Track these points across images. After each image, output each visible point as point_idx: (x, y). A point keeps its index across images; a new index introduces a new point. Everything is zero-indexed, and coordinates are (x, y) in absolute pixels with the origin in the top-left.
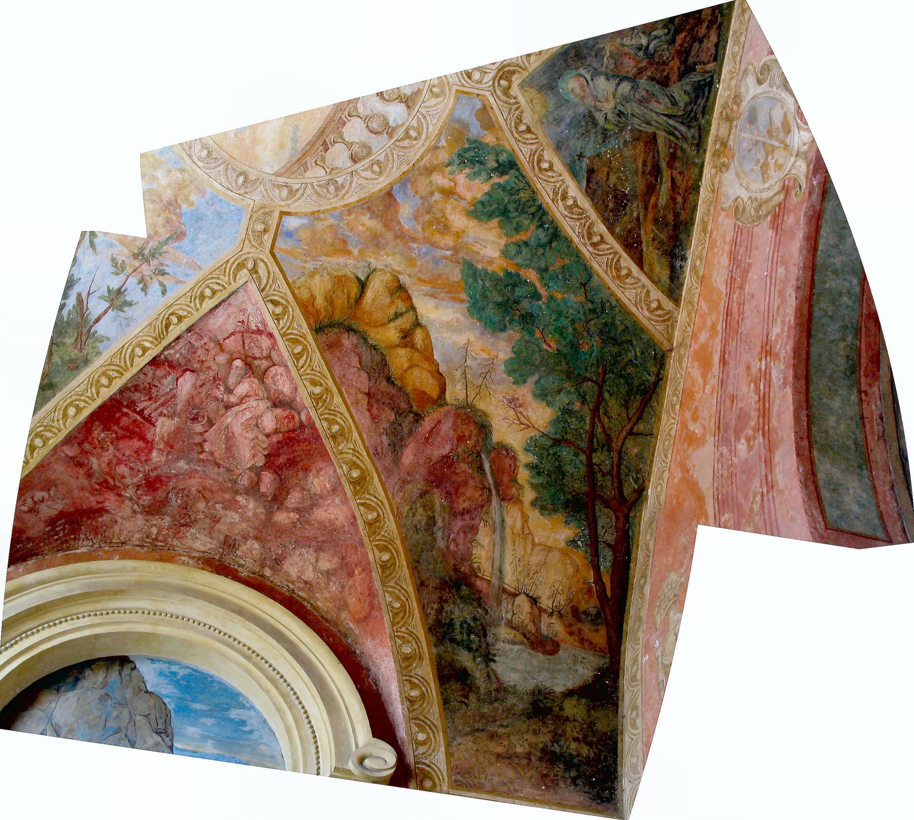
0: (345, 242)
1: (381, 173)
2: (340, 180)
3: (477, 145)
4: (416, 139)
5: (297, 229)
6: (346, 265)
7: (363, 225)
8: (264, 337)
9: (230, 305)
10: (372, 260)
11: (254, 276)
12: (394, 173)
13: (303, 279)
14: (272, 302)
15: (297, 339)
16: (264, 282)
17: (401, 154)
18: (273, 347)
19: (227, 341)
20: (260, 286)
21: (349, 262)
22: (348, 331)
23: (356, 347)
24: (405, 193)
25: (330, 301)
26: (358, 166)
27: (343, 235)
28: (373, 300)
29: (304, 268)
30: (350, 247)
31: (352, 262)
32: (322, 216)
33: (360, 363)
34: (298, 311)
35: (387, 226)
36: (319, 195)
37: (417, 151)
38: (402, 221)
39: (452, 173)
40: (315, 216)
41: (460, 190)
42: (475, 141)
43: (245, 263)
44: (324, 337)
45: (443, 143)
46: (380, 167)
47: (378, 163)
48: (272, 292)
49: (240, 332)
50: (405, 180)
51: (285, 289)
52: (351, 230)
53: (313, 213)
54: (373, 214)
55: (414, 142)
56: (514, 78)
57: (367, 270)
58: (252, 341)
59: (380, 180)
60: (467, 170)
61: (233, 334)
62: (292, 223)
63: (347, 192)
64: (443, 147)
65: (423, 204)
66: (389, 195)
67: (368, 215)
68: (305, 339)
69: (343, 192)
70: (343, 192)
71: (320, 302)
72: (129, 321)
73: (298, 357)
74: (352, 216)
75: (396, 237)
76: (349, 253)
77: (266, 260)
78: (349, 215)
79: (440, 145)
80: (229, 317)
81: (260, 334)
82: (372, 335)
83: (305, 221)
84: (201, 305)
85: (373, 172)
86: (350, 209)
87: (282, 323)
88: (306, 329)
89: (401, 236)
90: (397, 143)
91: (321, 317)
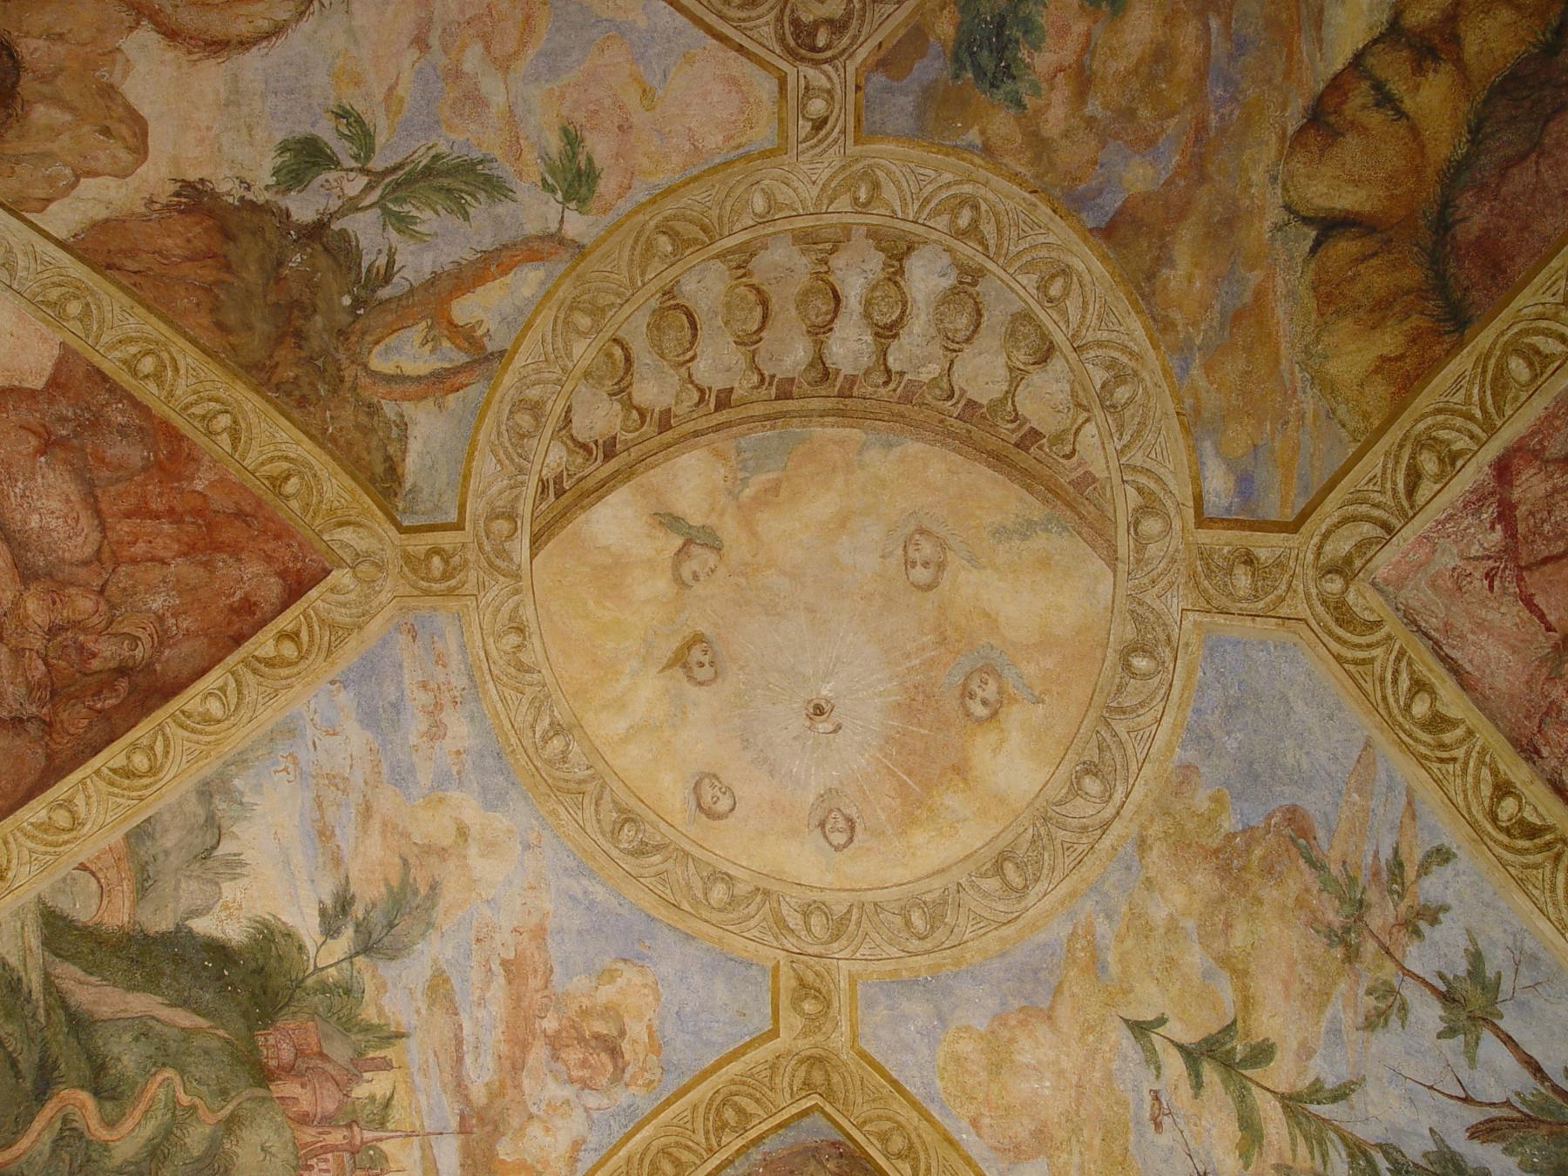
0: (1238, 316)
1: (1066, 272)
2: (1099, 376)
3: (964, 52)
4: (975, 207)
5: (1230, 464)
6: (1291, 294)
7: (1190, 279)
8: (1516, 495)
9: (1447, 627)
10: (1267, 224)
11: (1358, 563)
12: (1062, 238)
13: (1342, 410)
14: (1411, 491)
15: (1495, 379)
16: (1367, 529)
17: (1014, 234)
18: (1537, 454)
19: (1551, 618)
20: (1378, 540)
21: (1281, 289)
22: (1447, 228)
23: (1483, 187)
24: (1100, 192)
25: (1381, 310)
26: (1059, 338)
27: (1222, 328)
28: (1357, 183)
29: (1316, 416)
30: (1247, 298)
31: (1279, 281)
32: (1189, 402)
33: (1523, 157)
34: (1425, 400)
35: (1182, 215)
36: (1142, 424)
37: (1002, 195)
38: (1164, 176)
39: (1036, 92)
40: (1193, 422)
41: (1068, 55)
42: (956, 59)
43: (1332, 601)
44: (1475, 295)
45: (973, 135)
46: (1053, 277)
47: (1043, 287)
48: (1387, 499)
49: (1520, 579)
50: (1071, 202)
51: (1374, 461)
52: (1208, 307)
53: (1186, 430)
54: (1163, 258)
55: (984, 207)
56: (807, 18)
57: (1291, 231)
58: (1536, 531)
59: (1080, 267)
60: (1023, 54)
61: (1529, 602)
62: (1218, 483)
63: (1124, 349)
64: (982, 132)
65: (1117, 136)
66: (1111, 233)
67: (1165, 272)
68: (1488, 356)
69: (1125, 359)
70: (1125, 359)
71: (1389, 341)
72: (1523, 959)
73: (1536, 359)
74: (1176, 315)
75: (1203, 178)
76: (1259, 295)
77: (1316, 540)
78: (1174, 325)
79: (978, 142)
80: (1481, 625)
81: (1513, 507)
82: (1445, 151)
83: (1207, 445)
84: (1453, 724)
85: (1066, 292)
86: (1160, 325)
87: (1462, 443)
88: (1463, 362)
89: (1197, 170)
90: (992, 249)
91: (1424, 323)
